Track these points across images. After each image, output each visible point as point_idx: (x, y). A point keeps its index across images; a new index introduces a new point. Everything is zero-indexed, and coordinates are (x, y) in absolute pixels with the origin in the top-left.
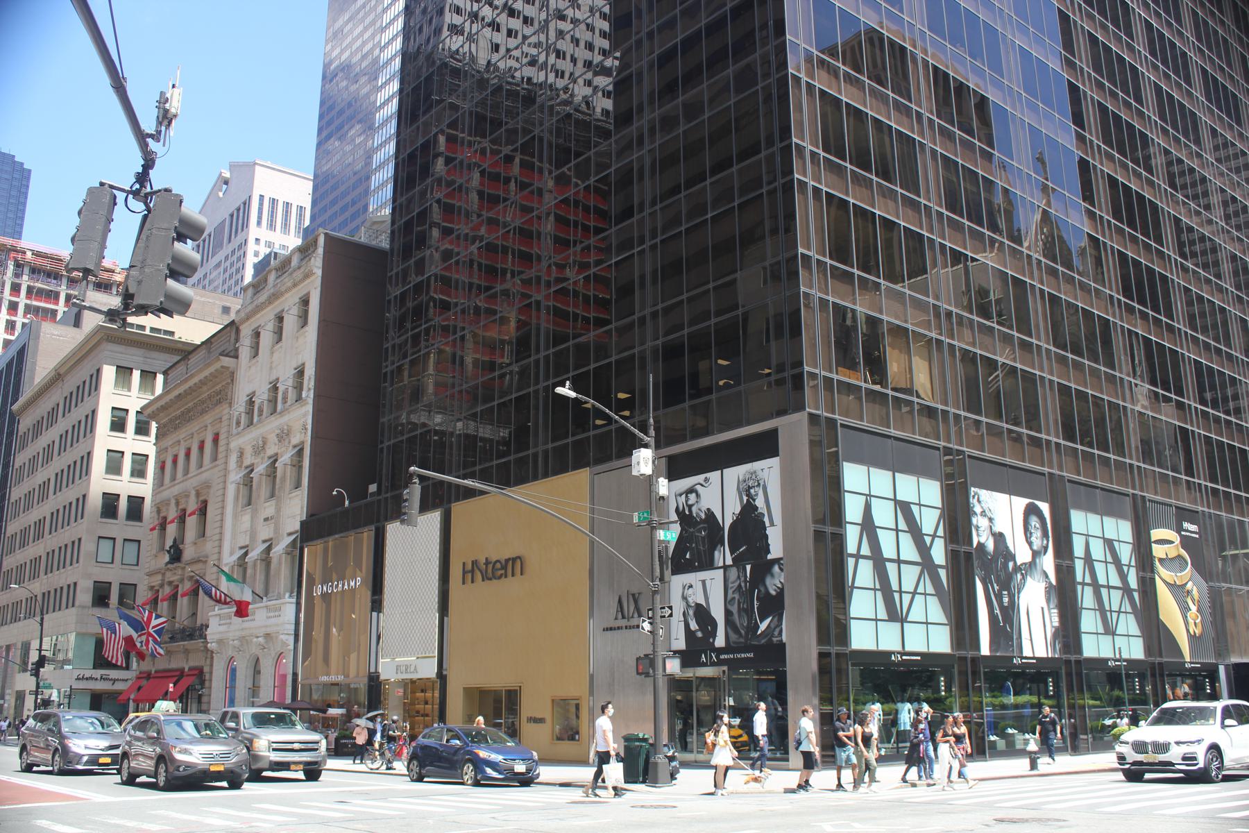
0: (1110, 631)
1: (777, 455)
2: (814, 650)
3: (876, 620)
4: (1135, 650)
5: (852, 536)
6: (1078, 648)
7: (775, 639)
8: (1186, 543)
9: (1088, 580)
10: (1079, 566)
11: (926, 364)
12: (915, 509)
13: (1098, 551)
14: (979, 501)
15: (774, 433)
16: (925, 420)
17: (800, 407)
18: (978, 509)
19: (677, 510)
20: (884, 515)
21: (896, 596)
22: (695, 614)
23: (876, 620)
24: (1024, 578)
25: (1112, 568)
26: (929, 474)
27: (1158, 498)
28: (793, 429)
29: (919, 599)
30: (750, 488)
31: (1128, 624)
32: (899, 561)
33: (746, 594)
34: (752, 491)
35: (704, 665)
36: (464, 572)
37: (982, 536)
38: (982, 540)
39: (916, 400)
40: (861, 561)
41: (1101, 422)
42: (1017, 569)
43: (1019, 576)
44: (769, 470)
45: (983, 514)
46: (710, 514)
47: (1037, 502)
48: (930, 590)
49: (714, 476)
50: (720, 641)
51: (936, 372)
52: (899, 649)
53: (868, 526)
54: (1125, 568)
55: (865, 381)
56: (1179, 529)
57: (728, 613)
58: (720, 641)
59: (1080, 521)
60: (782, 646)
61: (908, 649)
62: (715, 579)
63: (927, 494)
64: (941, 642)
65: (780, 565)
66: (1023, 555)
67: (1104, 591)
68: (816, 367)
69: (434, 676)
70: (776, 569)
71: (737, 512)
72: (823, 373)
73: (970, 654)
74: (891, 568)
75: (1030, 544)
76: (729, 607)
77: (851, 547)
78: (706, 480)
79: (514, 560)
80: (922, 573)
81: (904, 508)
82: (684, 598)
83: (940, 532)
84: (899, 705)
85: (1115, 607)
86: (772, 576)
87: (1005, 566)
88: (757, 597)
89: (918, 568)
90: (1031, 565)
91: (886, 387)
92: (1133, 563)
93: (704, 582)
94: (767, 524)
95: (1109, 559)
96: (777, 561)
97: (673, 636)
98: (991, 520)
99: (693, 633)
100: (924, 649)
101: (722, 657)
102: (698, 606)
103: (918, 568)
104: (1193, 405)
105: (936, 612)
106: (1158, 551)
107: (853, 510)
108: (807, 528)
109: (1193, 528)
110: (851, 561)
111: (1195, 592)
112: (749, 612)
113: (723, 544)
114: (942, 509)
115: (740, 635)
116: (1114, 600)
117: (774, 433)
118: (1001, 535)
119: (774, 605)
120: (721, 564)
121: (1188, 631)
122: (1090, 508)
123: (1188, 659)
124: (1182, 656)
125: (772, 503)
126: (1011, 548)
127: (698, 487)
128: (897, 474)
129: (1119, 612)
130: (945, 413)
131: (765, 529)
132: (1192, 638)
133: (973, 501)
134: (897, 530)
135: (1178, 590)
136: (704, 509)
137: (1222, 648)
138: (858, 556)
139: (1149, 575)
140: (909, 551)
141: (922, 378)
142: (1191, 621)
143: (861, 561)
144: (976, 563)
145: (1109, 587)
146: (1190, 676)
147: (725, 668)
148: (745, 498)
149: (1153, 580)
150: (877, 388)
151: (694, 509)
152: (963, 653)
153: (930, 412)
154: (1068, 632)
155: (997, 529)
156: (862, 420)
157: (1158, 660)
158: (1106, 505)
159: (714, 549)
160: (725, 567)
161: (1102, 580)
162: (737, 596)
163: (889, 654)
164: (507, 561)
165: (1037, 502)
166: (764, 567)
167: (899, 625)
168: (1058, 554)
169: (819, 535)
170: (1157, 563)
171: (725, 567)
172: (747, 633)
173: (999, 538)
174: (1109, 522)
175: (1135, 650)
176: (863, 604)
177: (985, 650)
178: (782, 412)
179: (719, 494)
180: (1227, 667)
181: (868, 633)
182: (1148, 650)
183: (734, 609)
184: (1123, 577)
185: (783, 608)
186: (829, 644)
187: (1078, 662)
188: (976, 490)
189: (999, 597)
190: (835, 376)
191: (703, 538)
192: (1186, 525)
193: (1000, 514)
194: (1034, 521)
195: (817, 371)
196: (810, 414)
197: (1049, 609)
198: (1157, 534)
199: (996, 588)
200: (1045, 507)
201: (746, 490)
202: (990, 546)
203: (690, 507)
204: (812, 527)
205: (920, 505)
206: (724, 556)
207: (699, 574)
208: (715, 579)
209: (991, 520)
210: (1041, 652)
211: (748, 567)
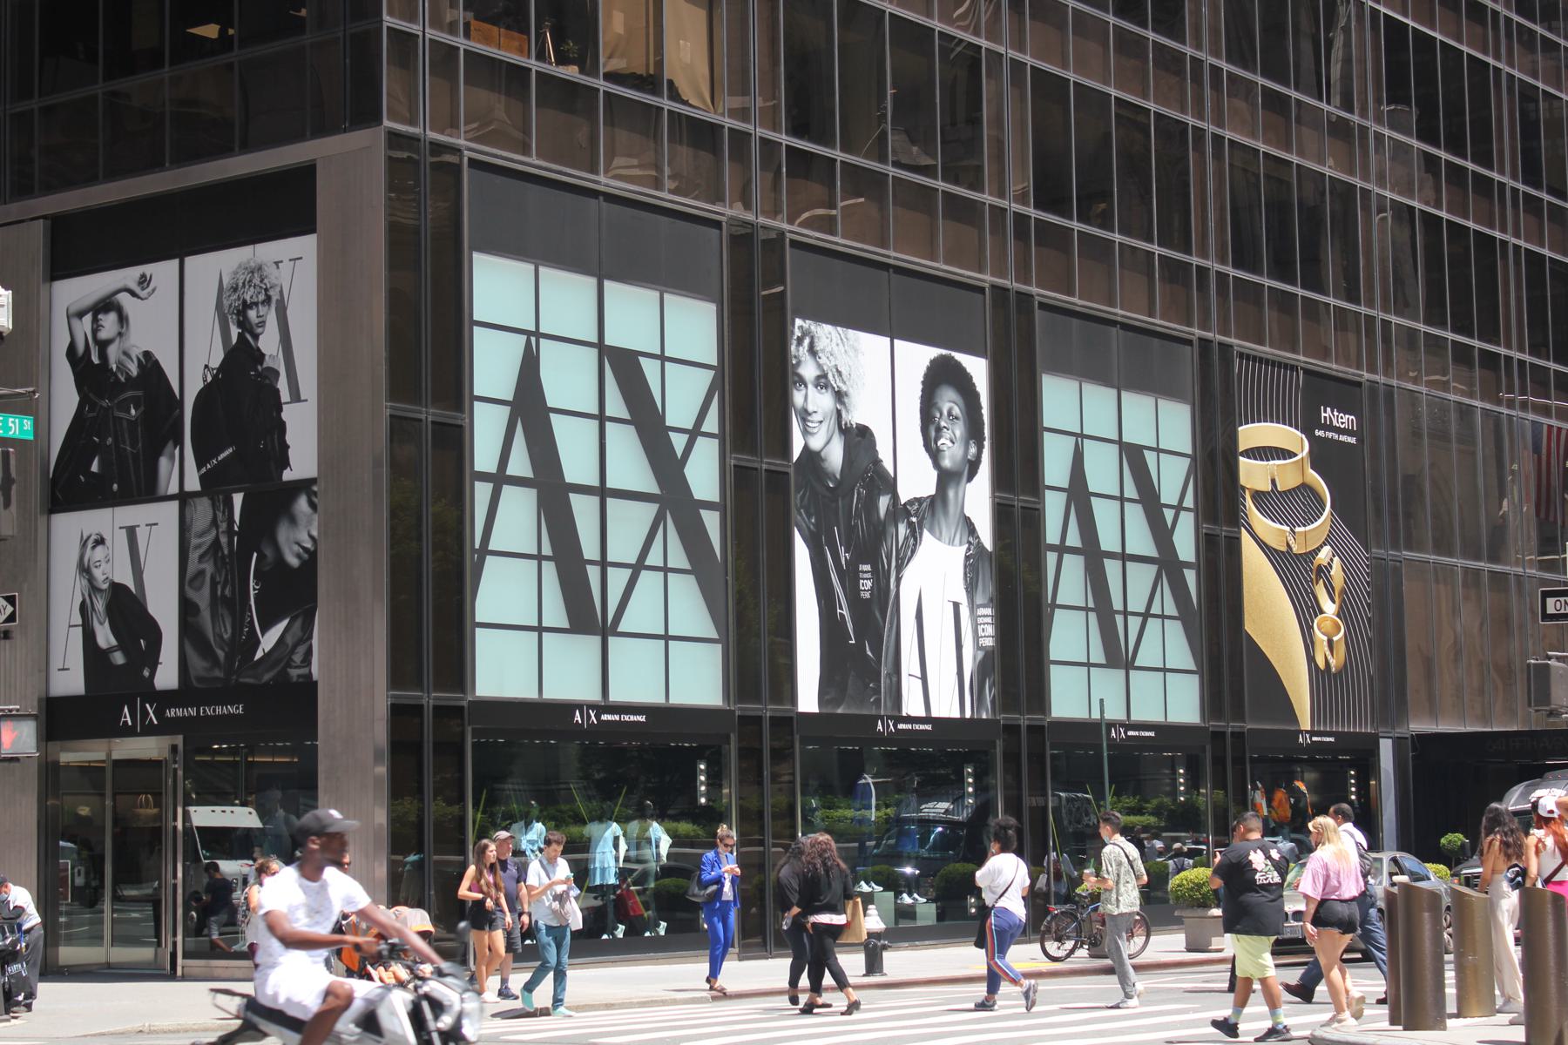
0: (1119, 657)
1: (313, 231)
2: (380, 701)
3: (540, 629)
4: (1183, 704)
5: (487, 432)
6: (1039, 694)
7: (294, 673)
8: (1323, 456)
9: (1073, 540)
10: (1054, 506)
11: (702, 14)
12: (650, 368)
13: (1103, 471)
14: (812, 351)
15: (306, 173)
16: (685, 151)
17: (376, 119)
18: (808, 371)
20: (569, 380)
21: (593, 573)
22: (110, 610)
23: (540, 629)
24: (915, 535)
25: (1135, 514)
26: (689, 285)
27: (1266, 350)
28: (350, 165)
29: (649, 583)
30: (246, 306)
31: (1167, 645)
32: (603, 492)
33: (229, 563)
34: (252, 314)
35: (129, 732)
37: (814, 435)
38: (816, 443)
39: (666, 104)
40: (507, 490)
41: (1135, 167)
42: (900, 511)
43: (903, 530)
44: (291, 262)
45: (822, 382)
46: (150, 364)
47: (958, 356)
48: (678, 558)
49: (163, 272)
50: (167, 676)
51: (723, 34)
52: (594, 695)
53: (529, 407)
54: (1169, 515)
55: (541, 56)
56: (1309, 425)
57: (187, 608)
58: (167, 676)
59: (1060, 400)
60: (309, 687)
61: (616, 696)
62: (158, 525)
63: (682, 334)
64: (699, 681)
65: (311, 495)
66: (915, 479)
67: (1112, 568)
68: (412, 18)
70: (302, 504)
71: (217, 359)
72: (431, 33)
73: (769, 710)
74: (583, 510)
75: (935, 454)
76: (191, 594)
77: (484, 456)
78: (144, 281)
80: (658, 520)
81: (622, 365)
82: (85, 570)
83: (711, 424)
84: (592, 829)
85: (1137, 603)
86: (293, 521)
87: (871, 505)
88: (251, 572)
89: (649, 511)
90: (934, 507)
91: (594, 72)
92: (1189, 502)
93: (131, 532)
94: (285, 396)
95: (1131, 491)
96: (305, 485)
97: (56, 662)
98: (840, 396)
99: (106, 654)
100: (654, 697)
101: (171, 713)
102: (117, 589)
103: (651, 509)
104: (1374, 127)
105: (690, 610)
106: (1253, 474)
107: (492, 367)
108: (375, 410)
109: (1345, 420)
110: (482, 491)
111: (1336, 571)
112: (233, 605)
113: (179, 442)
114: (719, 370)
116: (1136, 586)
117: (306, 173)
118: (864, 432)
119: (293, 592)
120: (173, 488)
121: (1311, 659)
122: (1091, 369)
123: (1305, 723)
124: (1291, 716)
125: (297, 343)
126: (888, 465)
127: (124, 298)
128: (609, 285)
129: (1146, 615)
130: (740, 138)
132: (1319, 677)
133: (799, 352)
134: (602, 418)
135: (1296, 571)
136: (136, 352)
137: (1391, 699)
138: (500, 479)
139: (1224, 531)
140: (629, 466)
141: (686, 54)
142: (1320, 637)
143: (507, 490)
144: (795, 498)
145: (1124, 557)
146: (1312, 763)
147: (179, 740)
148: (235, 332)
149: (1234, 546)
150: (571, 72)
151: (113, 352)
152: (752, 708)
153: (702, 135)
154: (1017, 659)
155: (855, 417)
156: (526, 150)
157: (1233, 726)
158: (1130, 364)
159: (159, 454)
160: (184, 498)
161: (1108, 540)
162: (209, 568)
163: (567, 708)
165: (958, 356)
166: (274, 499)
167: (596, 640)
168: (1001, 481)
169: (400, 428)
170: (1249, 503)
171: (184, 498)
173: (858, 439)
174: (1138, 407)
175: (1183, 704)
176: (507, 592)
177: (808, 700)
178: (323, 128)
179: (171, 316)
180: (1398, 743)
181: (517, 655)
182: (1212, 699)
183: (202, 598)
184: (1162, 533)
185: (314, 600)
186: (419, 685)
187: (1036, 731)
188: (807, 324)
189: (850, 578)
190: (461, 42)
191: (132, 424)
192: (1327, 414)
193: (868, 383)
194: (949, 401)
195: (415, 29)
196: (394, 138)
197: (973, 607)
198: (1252, 434)
199: (844, 556)
200: (977, 368)
201: (238, 312)
202: (835, 456)
203: (103, 345)
204: (386, 409)
205: (662, 358)
206: (181, 469)
207: (118, 509)
208: (158, 525)
209: (840, 396)
210: (947, 706)
211: (238, 499)
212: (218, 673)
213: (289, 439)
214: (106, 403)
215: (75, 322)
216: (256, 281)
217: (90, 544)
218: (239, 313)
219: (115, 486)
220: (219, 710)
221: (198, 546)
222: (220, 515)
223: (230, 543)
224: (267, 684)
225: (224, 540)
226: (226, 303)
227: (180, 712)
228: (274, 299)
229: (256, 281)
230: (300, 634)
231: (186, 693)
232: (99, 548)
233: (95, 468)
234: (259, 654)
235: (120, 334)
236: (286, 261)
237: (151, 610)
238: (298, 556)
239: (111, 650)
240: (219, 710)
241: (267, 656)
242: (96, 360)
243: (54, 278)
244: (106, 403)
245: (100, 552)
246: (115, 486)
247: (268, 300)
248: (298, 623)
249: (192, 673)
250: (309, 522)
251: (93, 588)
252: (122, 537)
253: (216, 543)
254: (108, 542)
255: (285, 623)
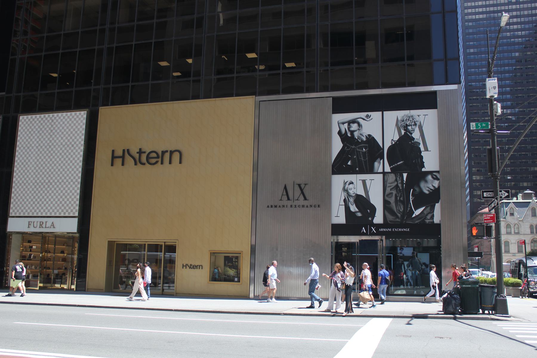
19: (340, 133)
36: (114, 157)
46: (371, 139)
50: (379, 219)
57: (386, 203)
58: (379, 219)
69: (76, 231)
70: (429, 177)
71: (397, 138)
76: (387, 198)
78: (367, 116)
79: (172, 153)
82: (345, 190)
86: (426, 181)
93: (364, 182)
96: (431, 173)
99: (354, 213)
115: (397, 217)
120: (381, 170)
127: (360, 121)
131: (420, 152)
148: (403, 132)
159: (375, 161)
160: (384, 173)
162: (394, 192)
164: (163, 153)
171: (384, 173)
172: (403, 216)
179: (381, 127)
183: (392, 200)
191: (364, 153)
201: (405, 128)
206: (383, 165)
211: (405, 175)
212: (398, 220)
213: (424, 160)
214: (353, 147)
215: (341, 126)
216: (411, 119)
217: (347, 183)
218: (404, 127)
219: (357, 169)
220: (400, 230)
221: (390, 186)
222: (398, 179)
223: (402, 186)
224: (417, 223)
225: (400, 185)
226: (400, 124)
227: (385, 230)
228: (418, 124)
229: (411, 119)
230: (429, 211)
231: (386, 224)
232: (351, 185)
233: (349, 163)
234: (414, 216)
235: (359, 129)
236: (422, 115)
237: (372, 202)
238: (428, 191)
239: (356, 212)
240: (400, 230)
241: (416, 216)
242: (349, 135)
243: (333, 113)
244: (353, 147)
245: (351, 186)
246: (357, 169)
247: (415, 125)
248: (429, 208)
249: (388, 220)
250: (432, 182)
251: (349, 195)
252: (360, 183)
253: (397, 186)
254: (355, 183)
255: (424, 208)
